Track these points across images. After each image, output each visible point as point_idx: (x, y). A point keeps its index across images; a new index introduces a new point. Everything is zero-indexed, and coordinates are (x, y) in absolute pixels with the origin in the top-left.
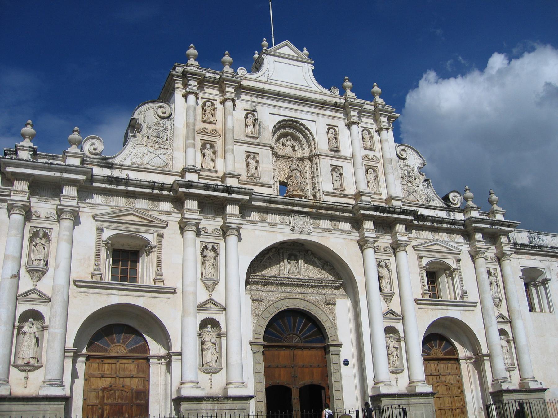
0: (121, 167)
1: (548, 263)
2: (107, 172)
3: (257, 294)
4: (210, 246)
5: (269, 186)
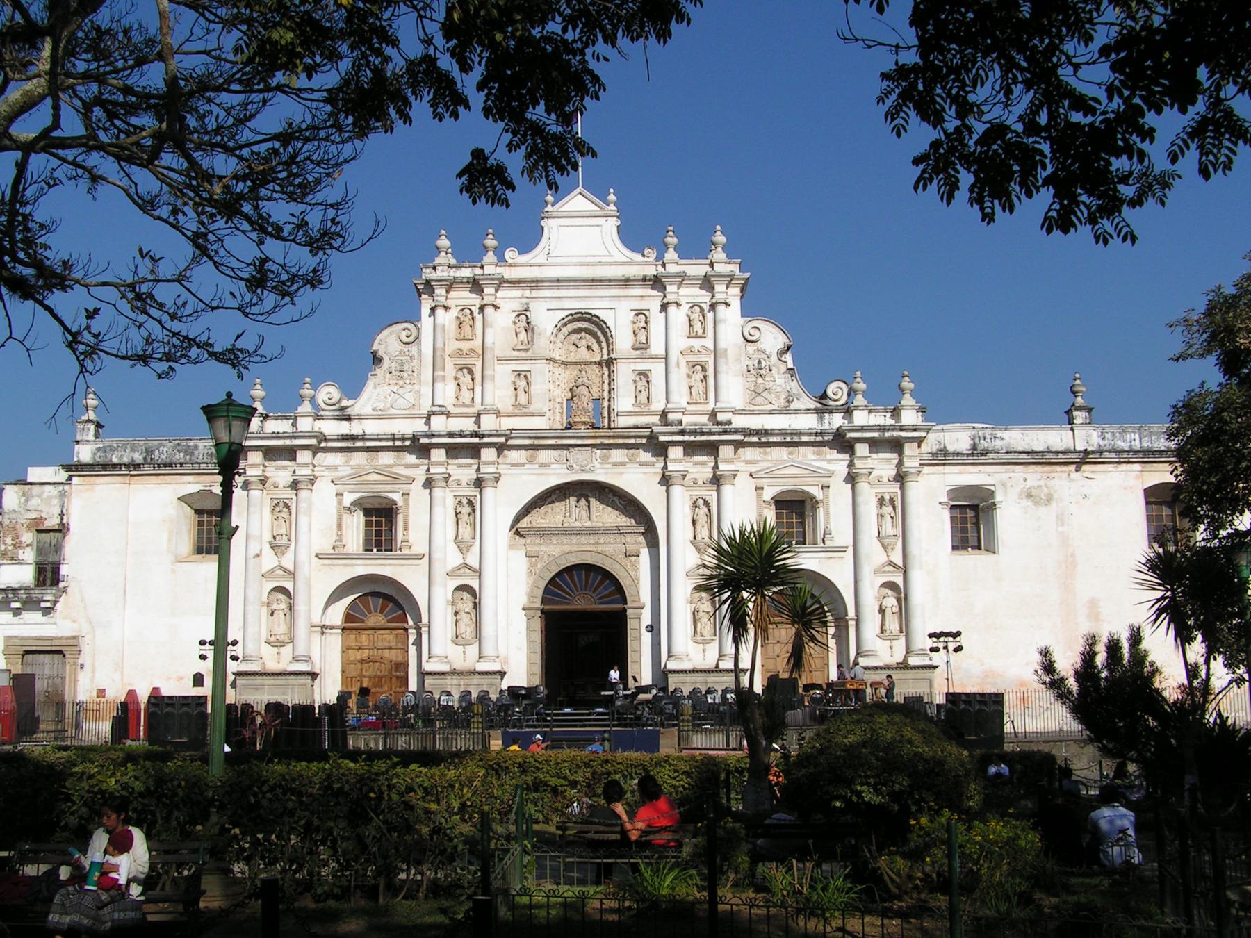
0: (360, 418)
1: (1004, 476)
2: (344, 428)
3: (533, 549)
4: (465, 501)
5: (542, 415)
